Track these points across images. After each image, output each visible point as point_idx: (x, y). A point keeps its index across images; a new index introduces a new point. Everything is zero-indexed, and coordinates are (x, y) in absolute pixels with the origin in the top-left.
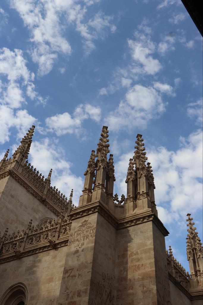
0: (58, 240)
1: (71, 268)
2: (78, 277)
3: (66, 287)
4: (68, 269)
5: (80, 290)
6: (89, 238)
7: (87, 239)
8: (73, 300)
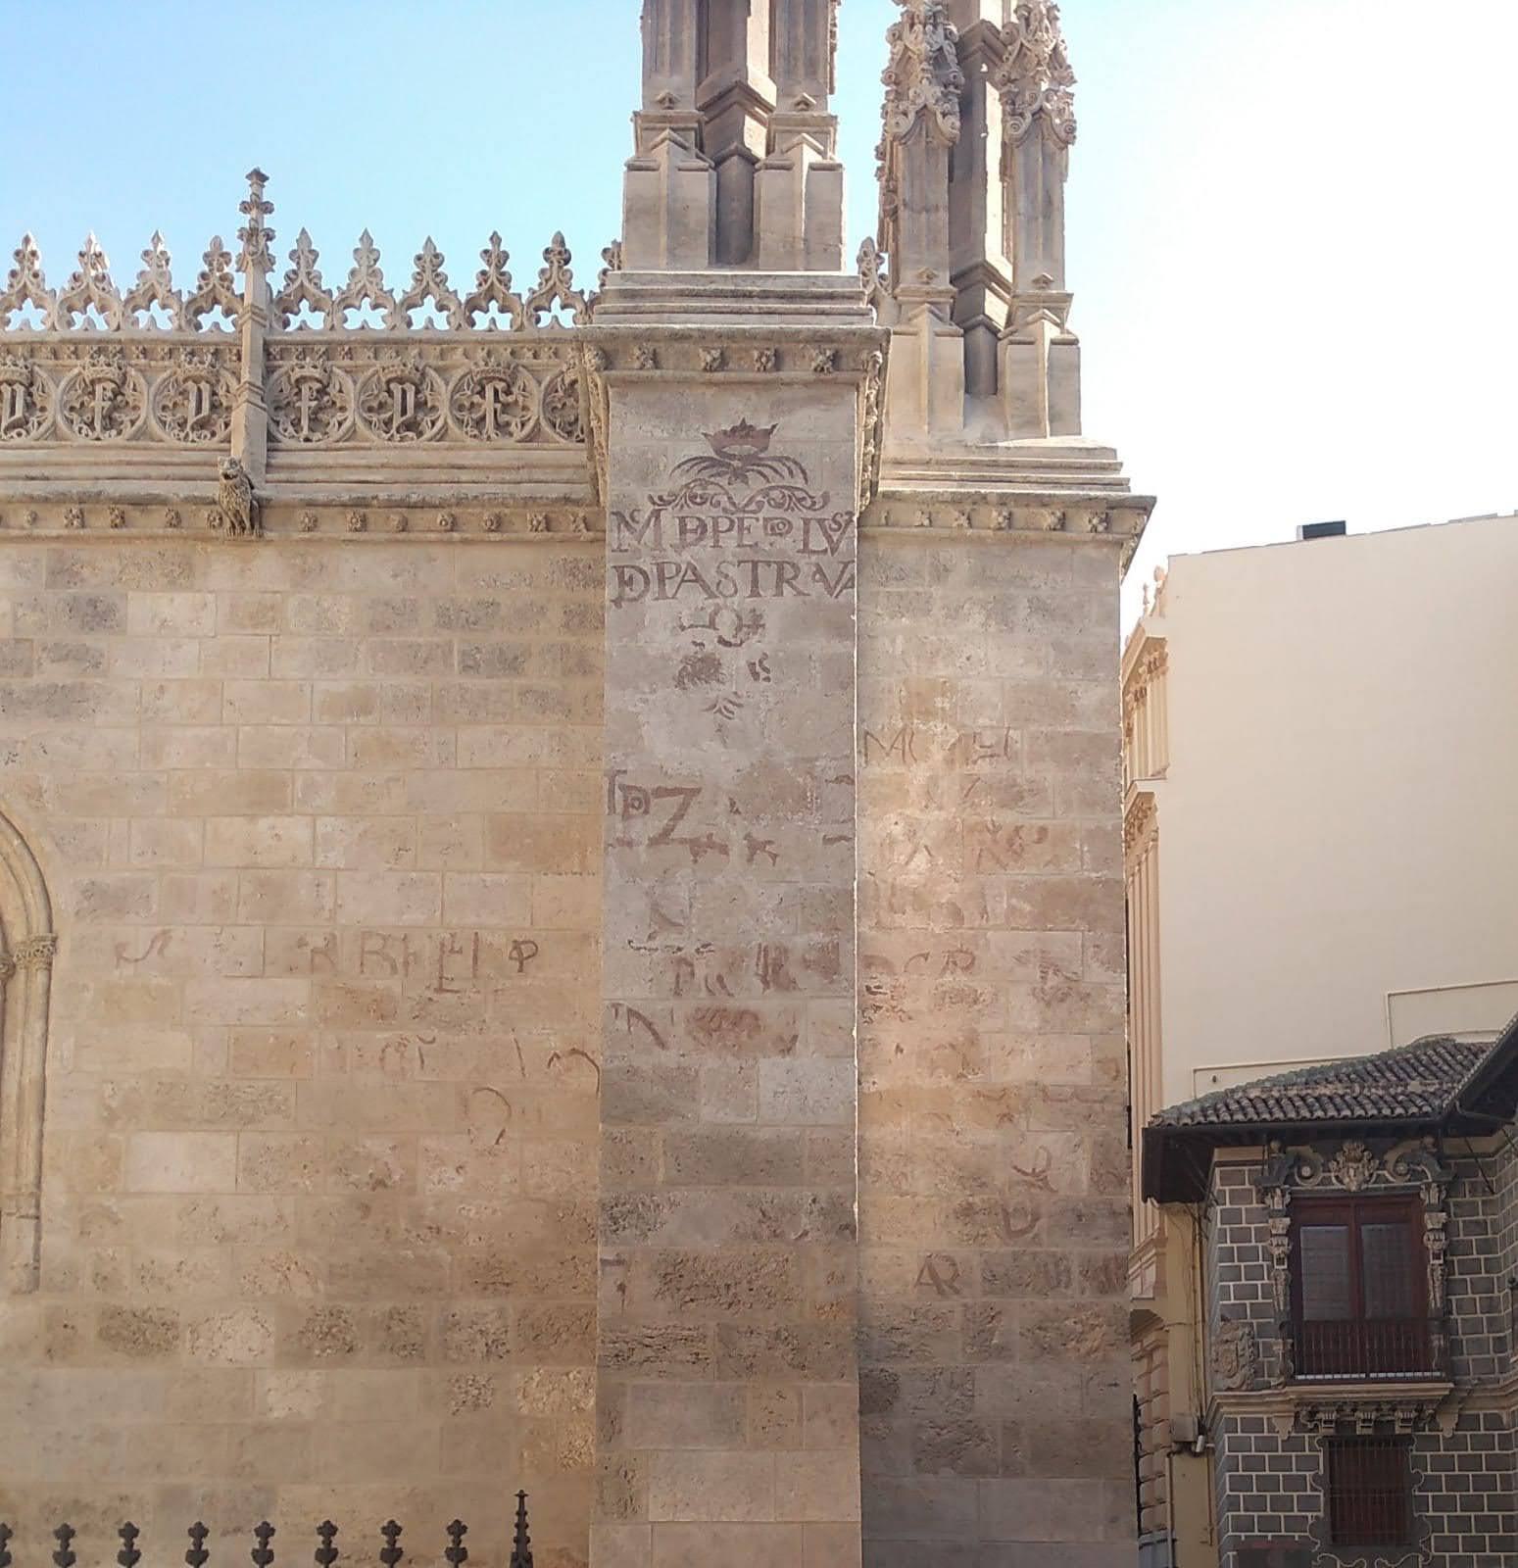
0: (268, 465)
1: (670, 784)
2: (750, 860)
3: (655, 908)
4: (649, 785)
5: (784, 951)
6: (798, 583)
7: (786, 589)
8: (733, 1004)
